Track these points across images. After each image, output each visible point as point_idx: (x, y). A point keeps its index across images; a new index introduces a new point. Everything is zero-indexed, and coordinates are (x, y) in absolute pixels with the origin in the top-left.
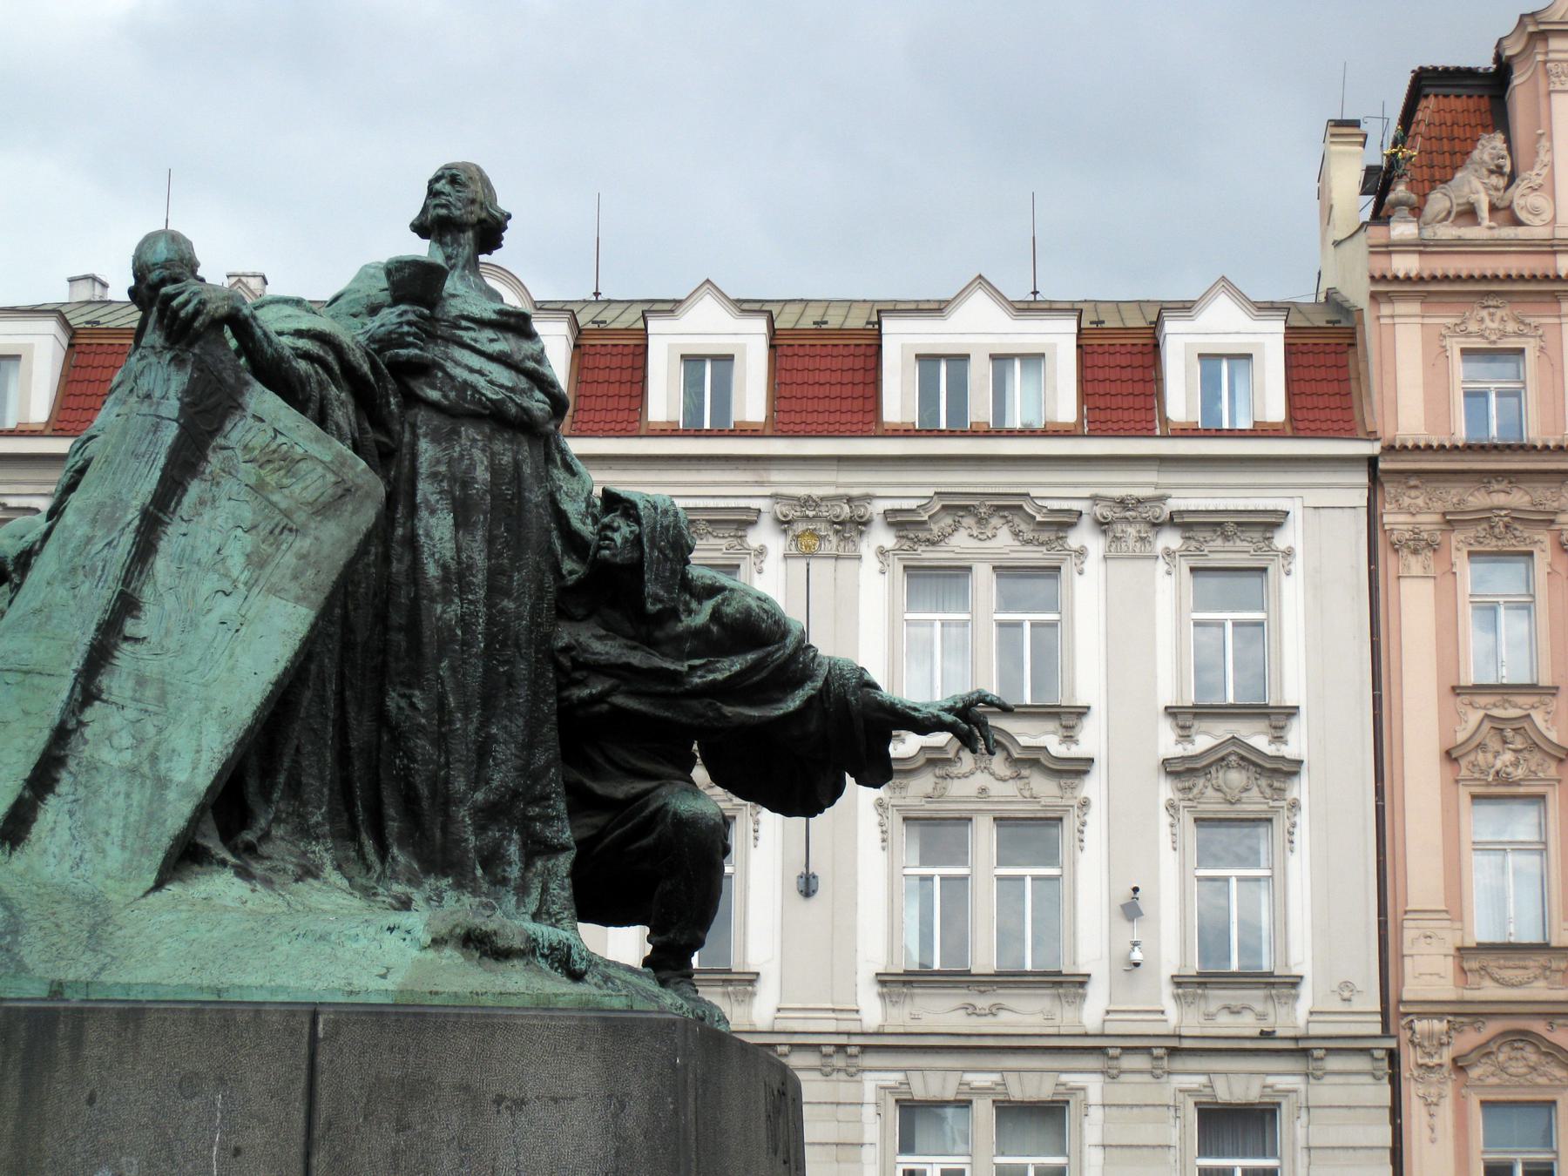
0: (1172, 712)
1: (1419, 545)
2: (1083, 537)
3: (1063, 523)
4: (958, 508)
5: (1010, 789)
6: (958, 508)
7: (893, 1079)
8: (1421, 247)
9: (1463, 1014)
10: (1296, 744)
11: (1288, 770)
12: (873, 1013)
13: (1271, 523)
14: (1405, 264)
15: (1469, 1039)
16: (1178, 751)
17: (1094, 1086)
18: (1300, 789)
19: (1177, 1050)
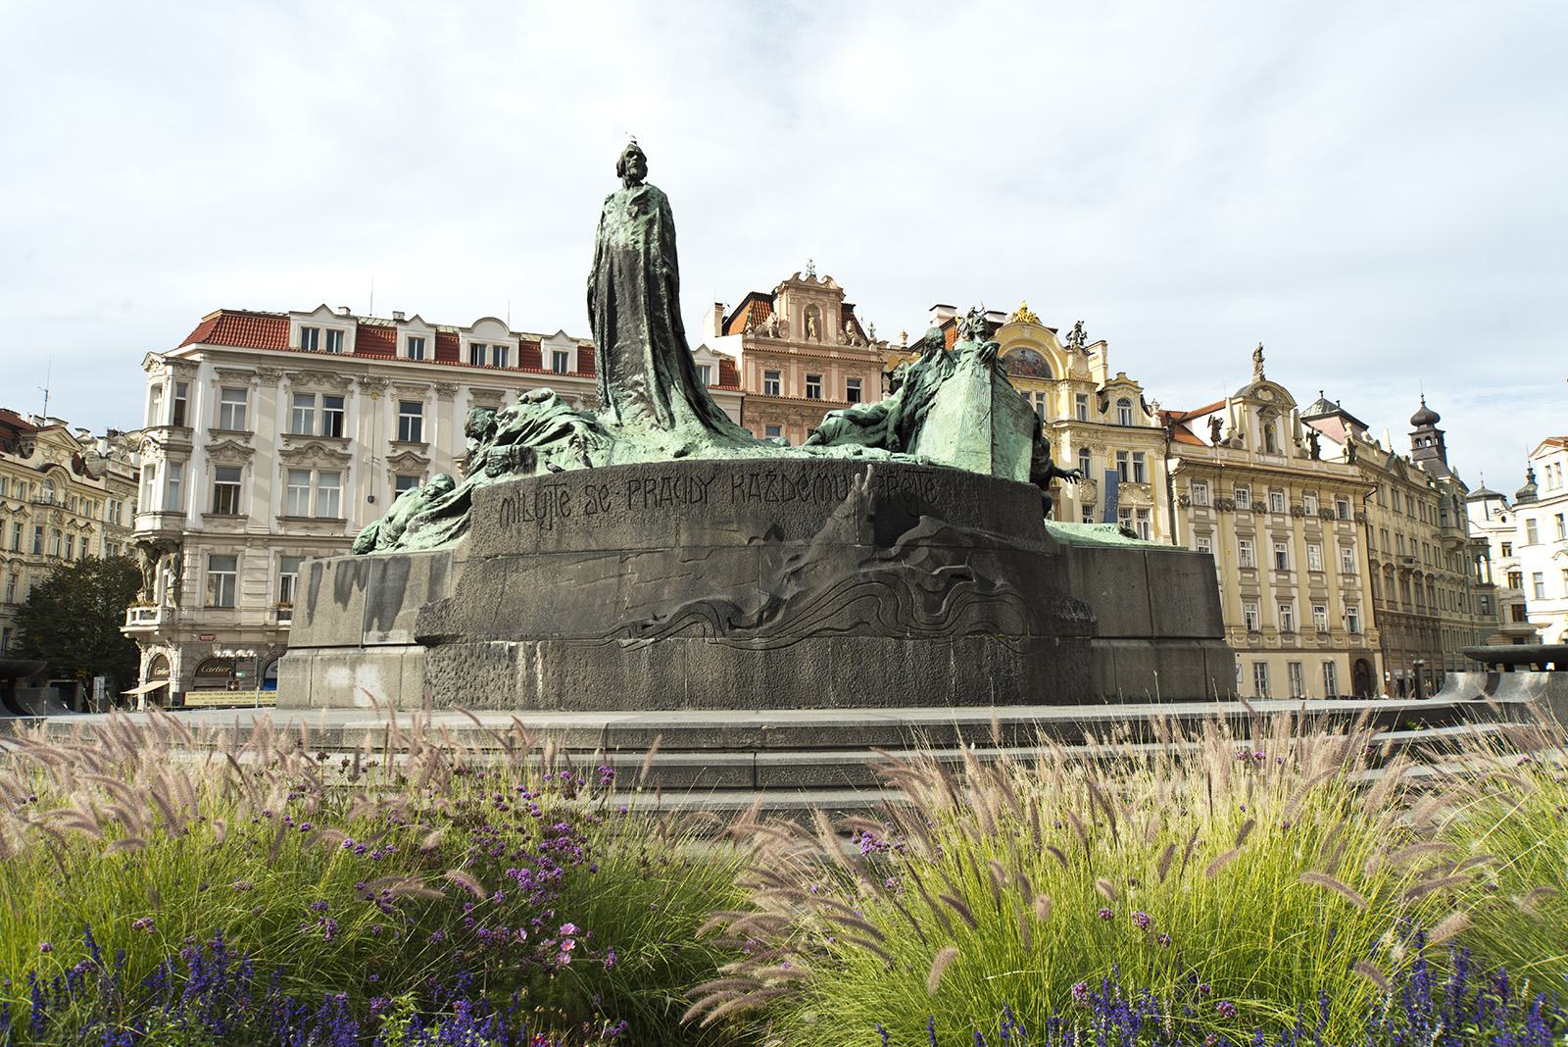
8: (756, 342)
14: (750, 346)
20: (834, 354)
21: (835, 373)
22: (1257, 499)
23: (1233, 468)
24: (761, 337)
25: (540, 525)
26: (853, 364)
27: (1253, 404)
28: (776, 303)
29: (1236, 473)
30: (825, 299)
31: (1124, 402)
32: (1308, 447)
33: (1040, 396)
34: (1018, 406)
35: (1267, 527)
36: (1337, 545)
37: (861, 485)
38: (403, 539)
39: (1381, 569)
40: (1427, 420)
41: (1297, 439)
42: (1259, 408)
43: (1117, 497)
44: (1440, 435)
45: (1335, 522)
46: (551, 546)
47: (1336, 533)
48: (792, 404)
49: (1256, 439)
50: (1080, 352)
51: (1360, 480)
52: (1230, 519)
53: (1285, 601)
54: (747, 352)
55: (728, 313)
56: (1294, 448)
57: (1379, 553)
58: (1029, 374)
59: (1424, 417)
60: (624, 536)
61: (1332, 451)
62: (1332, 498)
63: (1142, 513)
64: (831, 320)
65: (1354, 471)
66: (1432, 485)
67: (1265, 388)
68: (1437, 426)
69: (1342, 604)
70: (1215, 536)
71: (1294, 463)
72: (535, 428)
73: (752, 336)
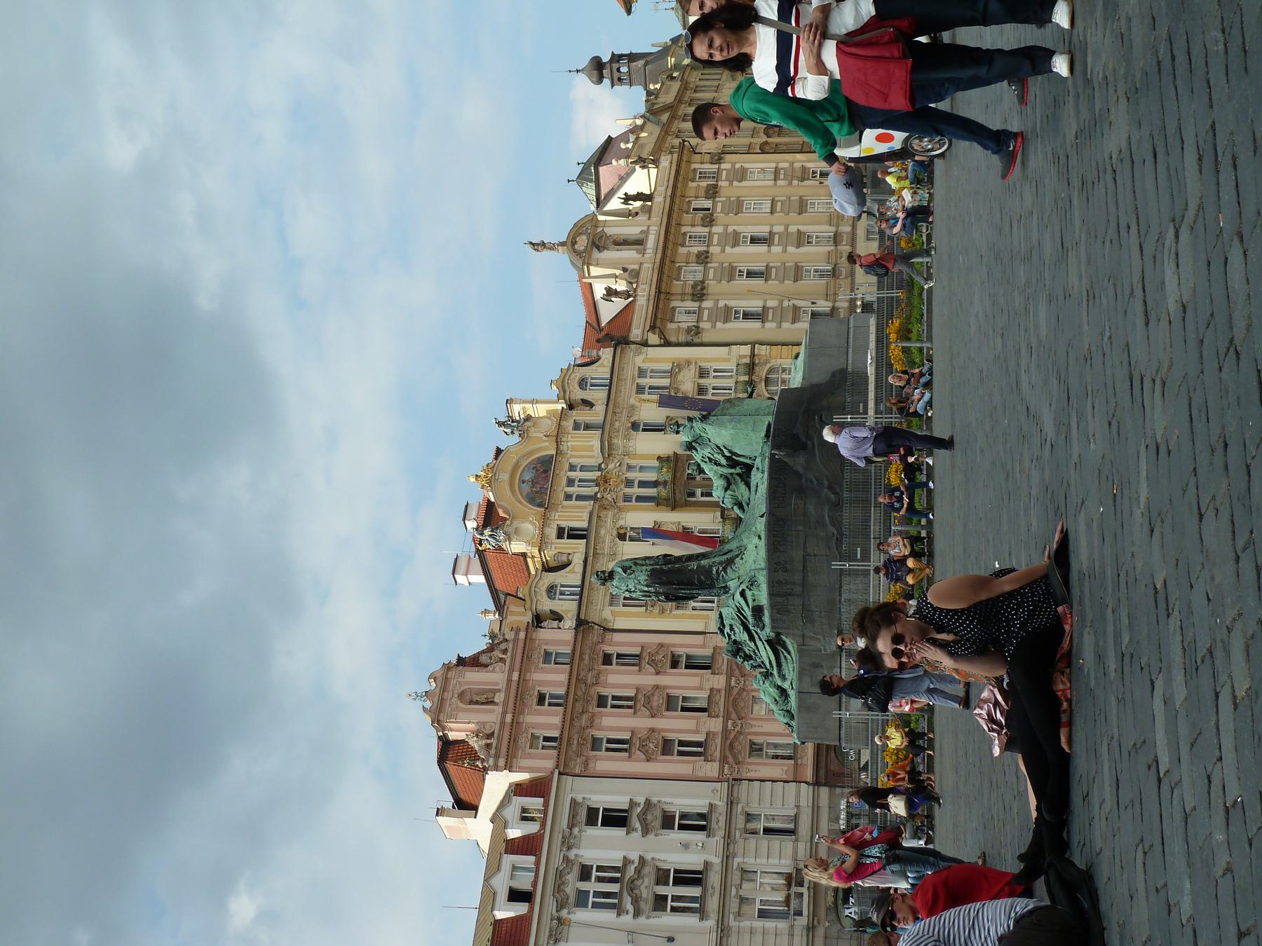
0: (628, 833)
1: (586, 764)
2: (572, 854)
3: (566, 859)
4: (559, 888)
5: (646, 880)
6: (559, 888)
7: (732, 917)
8: (497, 757)
9: (723, 760)
10: (641, 800)
11: (648, 802)
12: (711, 923)
13: (574, 803)
14: (502, 762)
15: (731, 759)
16: (640, 832)
17: (737, 860)
18: (654, 800)
19: (728, 838)
20: (515, 676)
21: (536, 676)
22: (693, 258)
23: (660, 281)
24: (493, 751)
25: (791, 595)
26: (526, 657)
27: (590, 256)
28: (452, 736)
29: (665, 278)
30: (453, 682)
31: (583, 383)
32: (638, 204)
33: (572, 468)
34: (728, 405)
35: (723, 251)
36: (744, 183)
37: (779, 454)
38: (786, 685)
39: (769, 140)
40: (598, 69)
41: (629, 214)
42: (595, 251)
43: (685, 398)
44: (616, 58)
45: (720, 183)
46: (798, 589)
47: (731, 184)
48: (569, 722)
49: (629, 254)
50: (528, 424)
51: (675, 156)
52: (712, 285)
53: (802, 239)
54: (509, 767)
55: (448, 801)
56: (638, 218)
57: (754, 140)
58: (546, 479)
59: (595, 73)
60: (797, 554)
61: (641, 181)
62: (694, 185)
63: (703, 373)
64: (474, 677)
65: (665, 161)
66: (675, 74)
67: (574, 243)
68: (606, 58)
69: (806, 183)
70: (731, 303)
71: (656, 219)
72: (739, 610)
73: (491, 761)
